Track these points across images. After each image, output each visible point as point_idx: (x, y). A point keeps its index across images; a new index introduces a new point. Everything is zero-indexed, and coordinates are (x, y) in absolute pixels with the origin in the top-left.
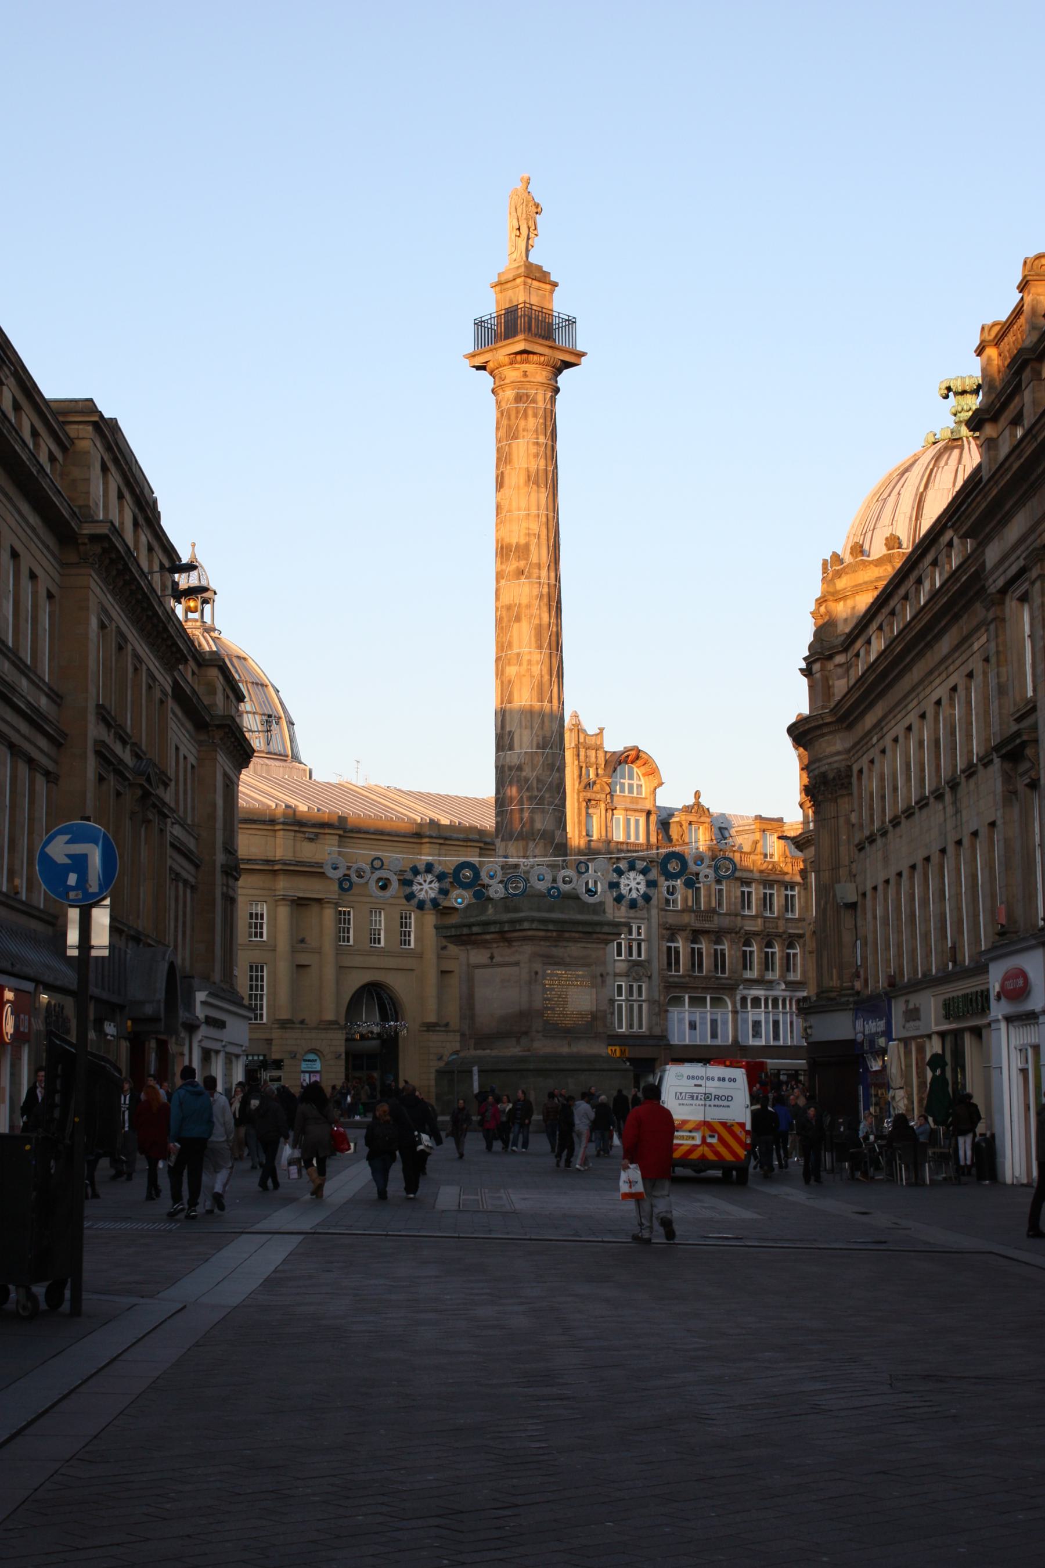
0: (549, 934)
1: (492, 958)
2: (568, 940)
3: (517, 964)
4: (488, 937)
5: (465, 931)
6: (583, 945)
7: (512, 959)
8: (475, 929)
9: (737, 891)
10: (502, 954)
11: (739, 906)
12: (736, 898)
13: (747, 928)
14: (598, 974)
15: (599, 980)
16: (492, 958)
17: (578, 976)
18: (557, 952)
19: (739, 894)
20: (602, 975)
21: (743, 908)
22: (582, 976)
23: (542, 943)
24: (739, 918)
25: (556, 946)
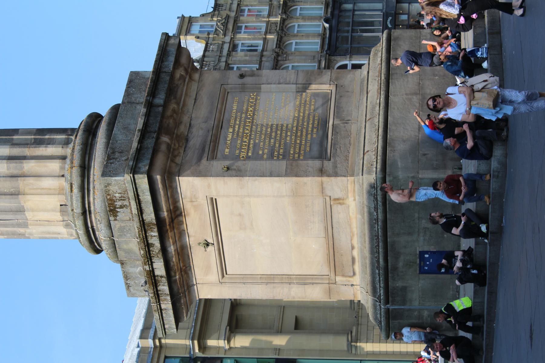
0: (163, 147)
1: (207, 244)
2: (178, 124)
3: (213, 202)
4: (172, 249)
5: (164, 288)
6: (190, 102)
7: (207, 209)
8: (160, 269)
9: (240, 55)
10: (196, 227)
11: (255, 53)
12: (246, 56)
13: (275, 46)
14: (240, 81)
15: (247, 80)
16: (207, 244)
17: (240, 110)
18: (197, 137)
19: (242, 54)
20: (242, 76)
21: (256, 50)
22: (241, 103)
23: (178, 160)
24: (265, 53)
25: (187, 140)
